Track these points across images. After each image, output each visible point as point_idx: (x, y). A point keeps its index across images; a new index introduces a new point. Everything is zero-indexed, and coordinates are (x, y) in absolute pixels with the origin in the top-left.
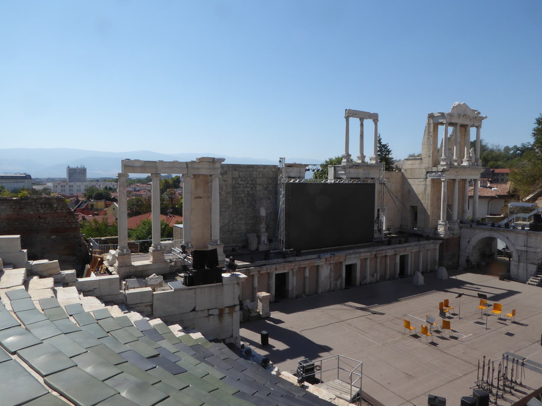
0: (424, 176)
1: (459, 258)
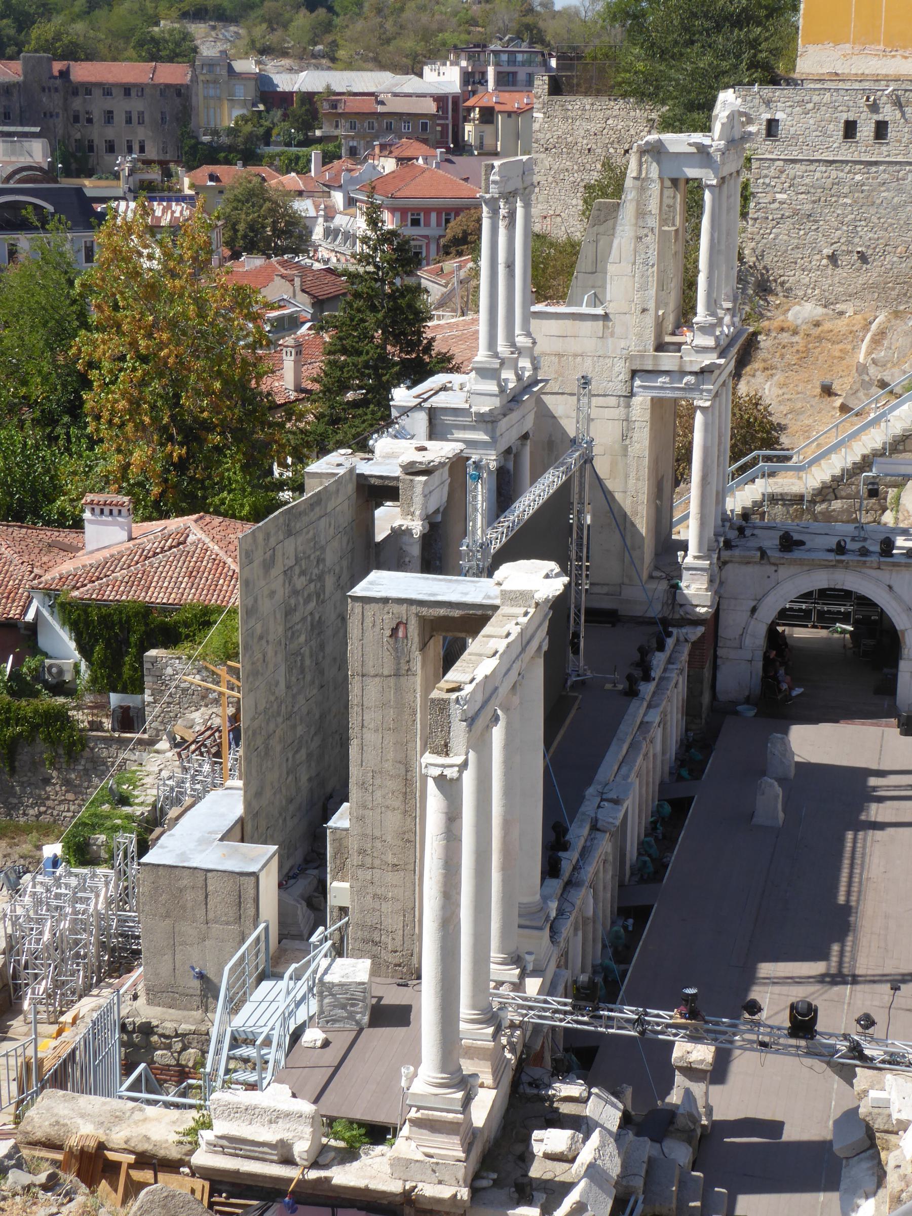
0: (621, 389)
1: (715, 668)
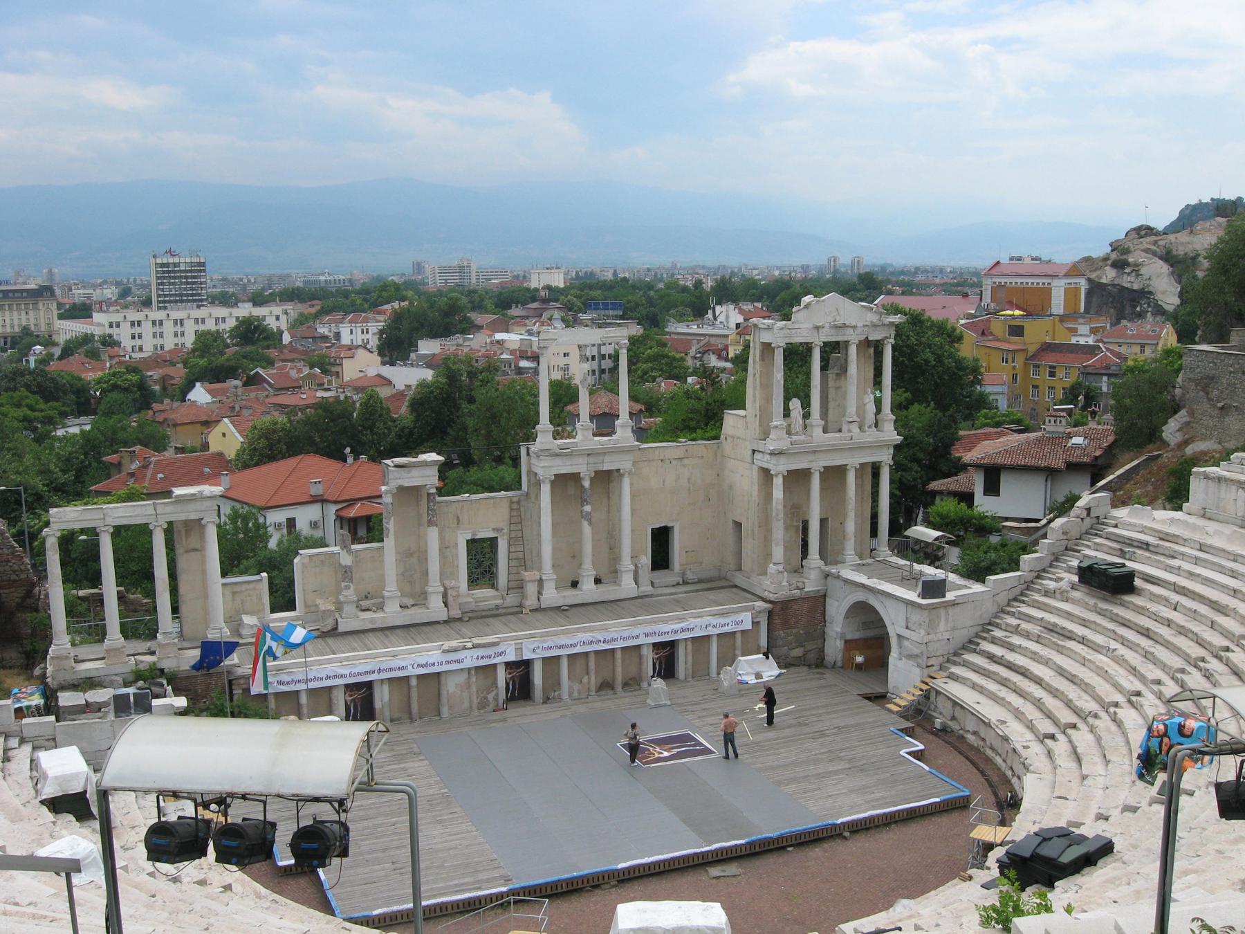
0: (749, 459)
